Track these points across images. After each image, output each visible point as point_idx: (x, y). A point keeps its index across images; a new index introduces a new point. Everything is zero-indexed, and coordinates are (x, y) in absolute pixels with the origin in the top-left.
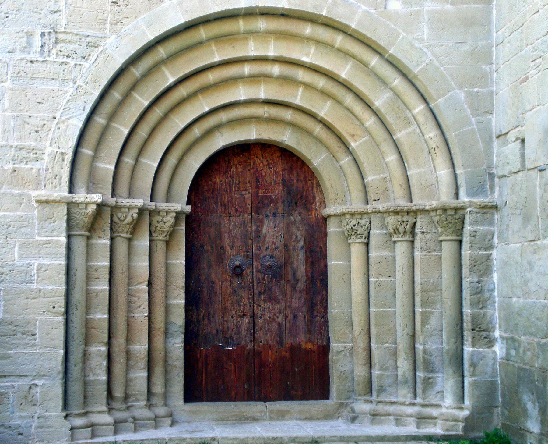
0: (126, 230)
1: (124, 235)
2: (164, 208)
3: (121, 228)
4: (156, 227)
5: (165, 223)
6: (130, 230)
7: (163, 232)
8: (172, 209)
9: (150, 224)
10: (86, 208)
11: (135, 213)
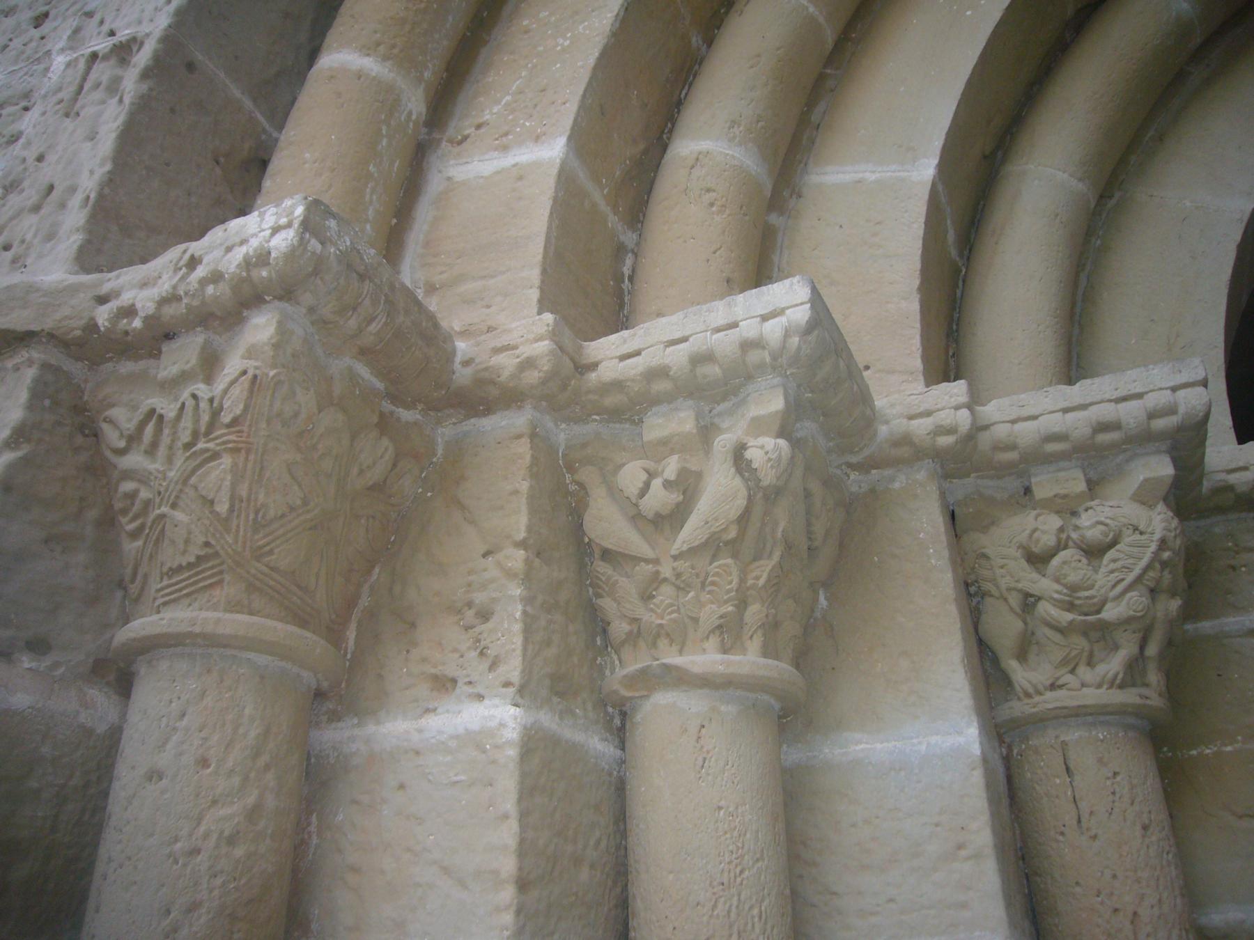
0: (710, 613)
1: (705, 658)
2: (1055, 423)
3: (665, 594)
4: (1029, 602)
5: (1094, 552)
6: (755, 612)
7: (1101, 634)
8: (1131, 413)
9: (973, 595)
10: (210, 363)
11: (758, 426)
